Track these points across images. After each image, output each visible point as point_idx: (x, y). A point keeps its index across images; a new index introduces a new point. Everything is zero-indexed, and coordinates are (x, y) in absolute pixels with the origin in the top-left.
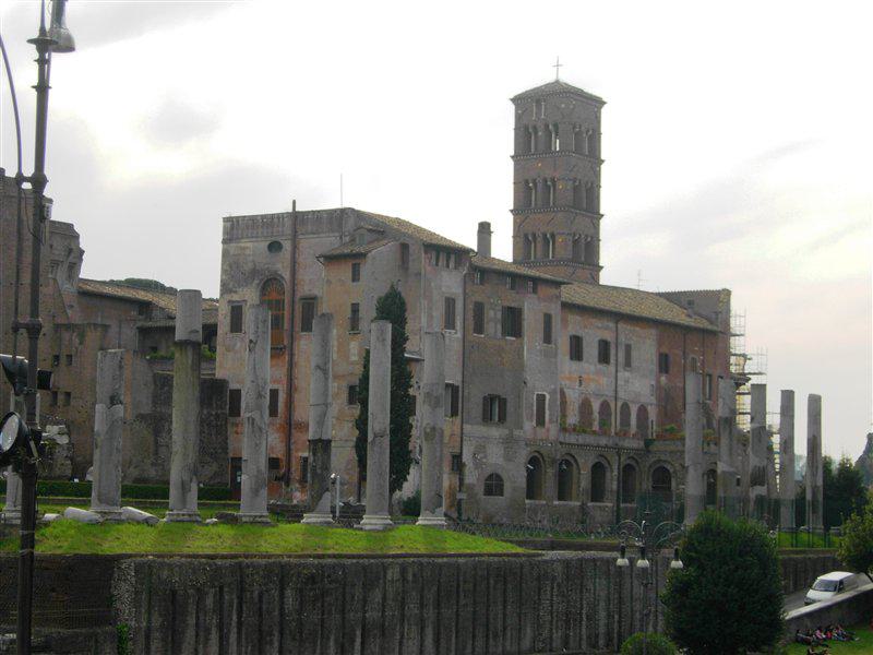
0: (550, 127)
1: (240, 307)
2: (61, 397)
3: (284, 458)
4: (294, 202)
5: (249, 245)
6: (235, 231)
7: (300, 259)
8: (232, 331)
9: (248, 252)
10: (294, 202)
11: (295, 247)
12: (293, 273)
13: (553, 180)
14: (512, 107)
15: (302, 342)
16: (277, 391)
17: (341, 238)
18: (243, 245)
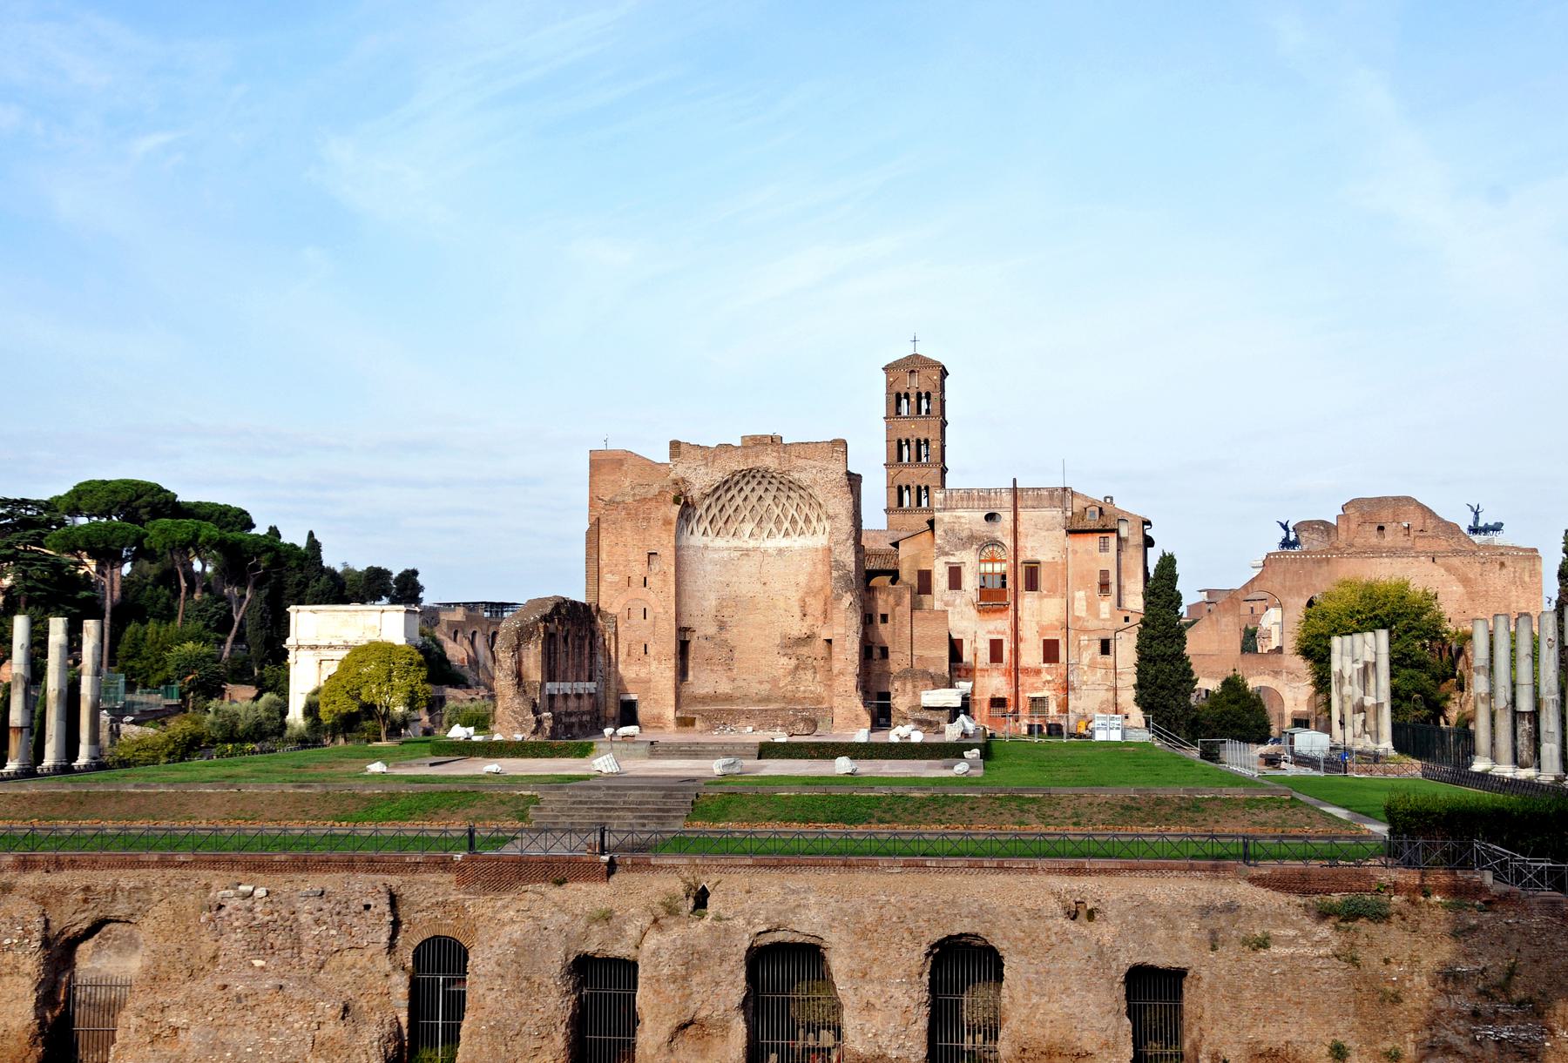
0: (923, 395)
1: (959, 568)
2: (876, 653)
3: (1013, 699)
4: (1015, 480)
5: (966, 514)
6: (949, 502)
7: (1020, 529)
8: (950, 589)
9: (963, 520)
10: (1015, 480)
11: (1015, 520)
13: (927, 441)
14: (883, 375)
15: (1026, 600)
16: (1000, 641)
18: (958, 514)
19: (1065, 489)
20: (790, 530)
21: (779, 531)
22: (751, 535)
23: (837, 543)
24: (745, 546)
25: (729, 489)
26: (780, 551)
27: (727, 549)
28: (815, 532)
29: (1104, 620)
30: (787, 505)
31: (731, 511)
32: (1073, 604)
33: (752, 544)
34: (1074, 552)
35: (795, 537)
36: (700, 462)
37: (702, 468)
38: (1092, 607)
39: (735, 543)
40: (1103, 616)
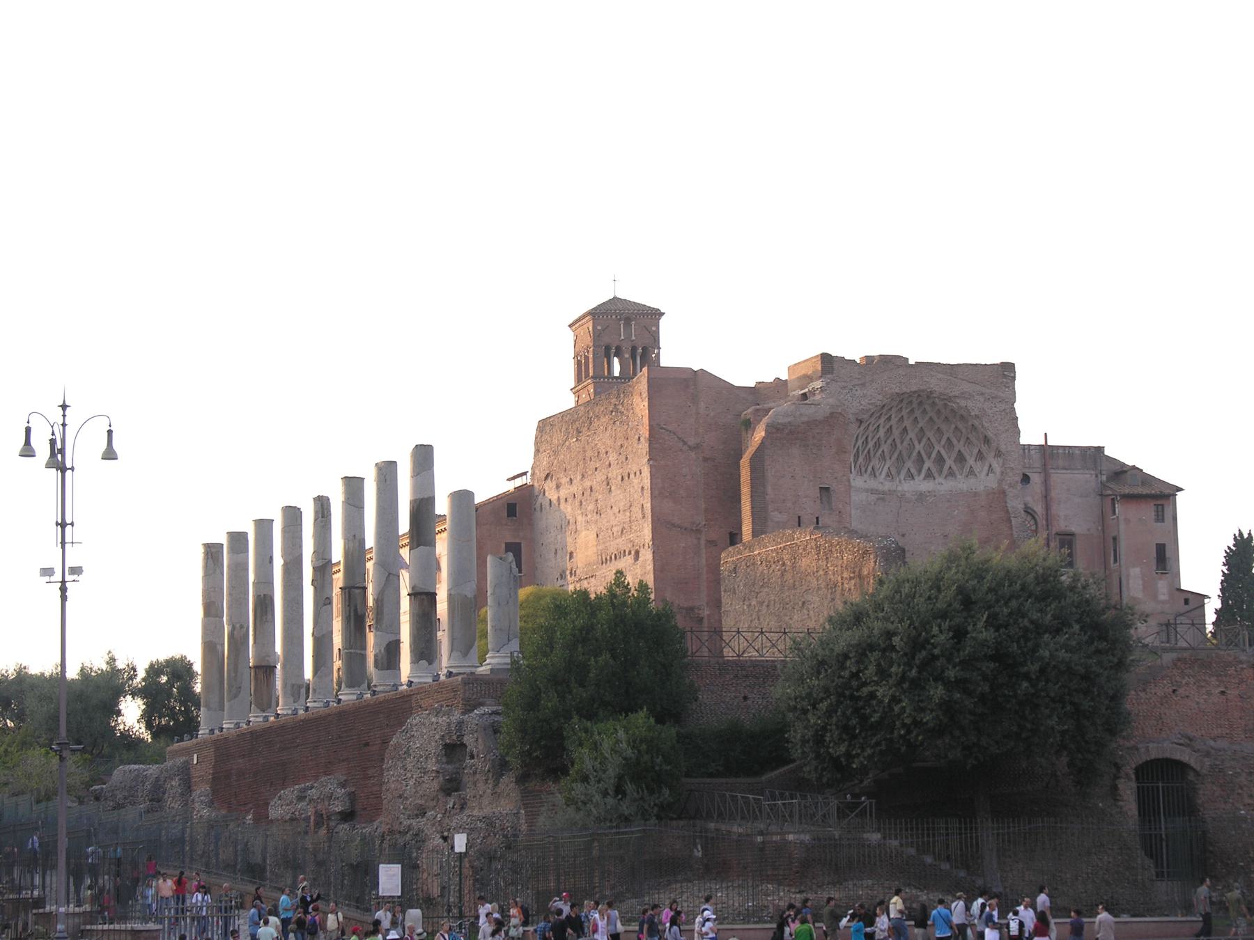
7: (1053, 494)
11: (1046, 482)
12: (1047, 508)
17: (1097, 476)
19: (1100, 450)
20: (934, 470)
21: (920, 472)
22: (888, 476)
23: (1011, 486)
24: (880, 488)
25: (879, 417)
26: (921, 497)
27: (867, 490)
28: (971, 472)
29: (1163, 602)
30: (933, 440)
31: (871, 444)
32: (1128, 583)
33: (888, 486)
34: (1127, 521)
35: (941, 480)
36: (856, 382)
37: (857, 388)
38: (1149, 587)
39: (873, 484)
40: (1162, 597)
